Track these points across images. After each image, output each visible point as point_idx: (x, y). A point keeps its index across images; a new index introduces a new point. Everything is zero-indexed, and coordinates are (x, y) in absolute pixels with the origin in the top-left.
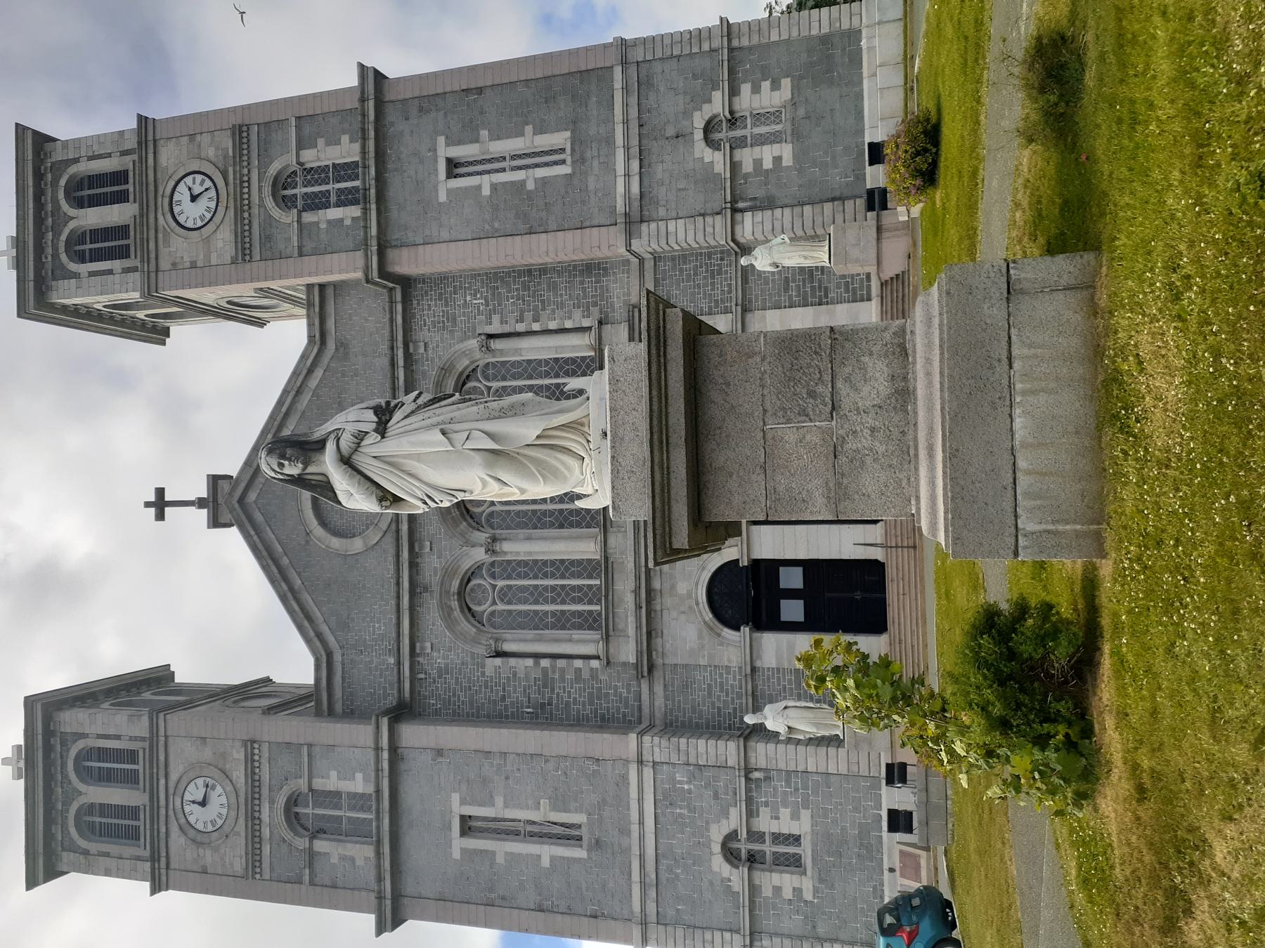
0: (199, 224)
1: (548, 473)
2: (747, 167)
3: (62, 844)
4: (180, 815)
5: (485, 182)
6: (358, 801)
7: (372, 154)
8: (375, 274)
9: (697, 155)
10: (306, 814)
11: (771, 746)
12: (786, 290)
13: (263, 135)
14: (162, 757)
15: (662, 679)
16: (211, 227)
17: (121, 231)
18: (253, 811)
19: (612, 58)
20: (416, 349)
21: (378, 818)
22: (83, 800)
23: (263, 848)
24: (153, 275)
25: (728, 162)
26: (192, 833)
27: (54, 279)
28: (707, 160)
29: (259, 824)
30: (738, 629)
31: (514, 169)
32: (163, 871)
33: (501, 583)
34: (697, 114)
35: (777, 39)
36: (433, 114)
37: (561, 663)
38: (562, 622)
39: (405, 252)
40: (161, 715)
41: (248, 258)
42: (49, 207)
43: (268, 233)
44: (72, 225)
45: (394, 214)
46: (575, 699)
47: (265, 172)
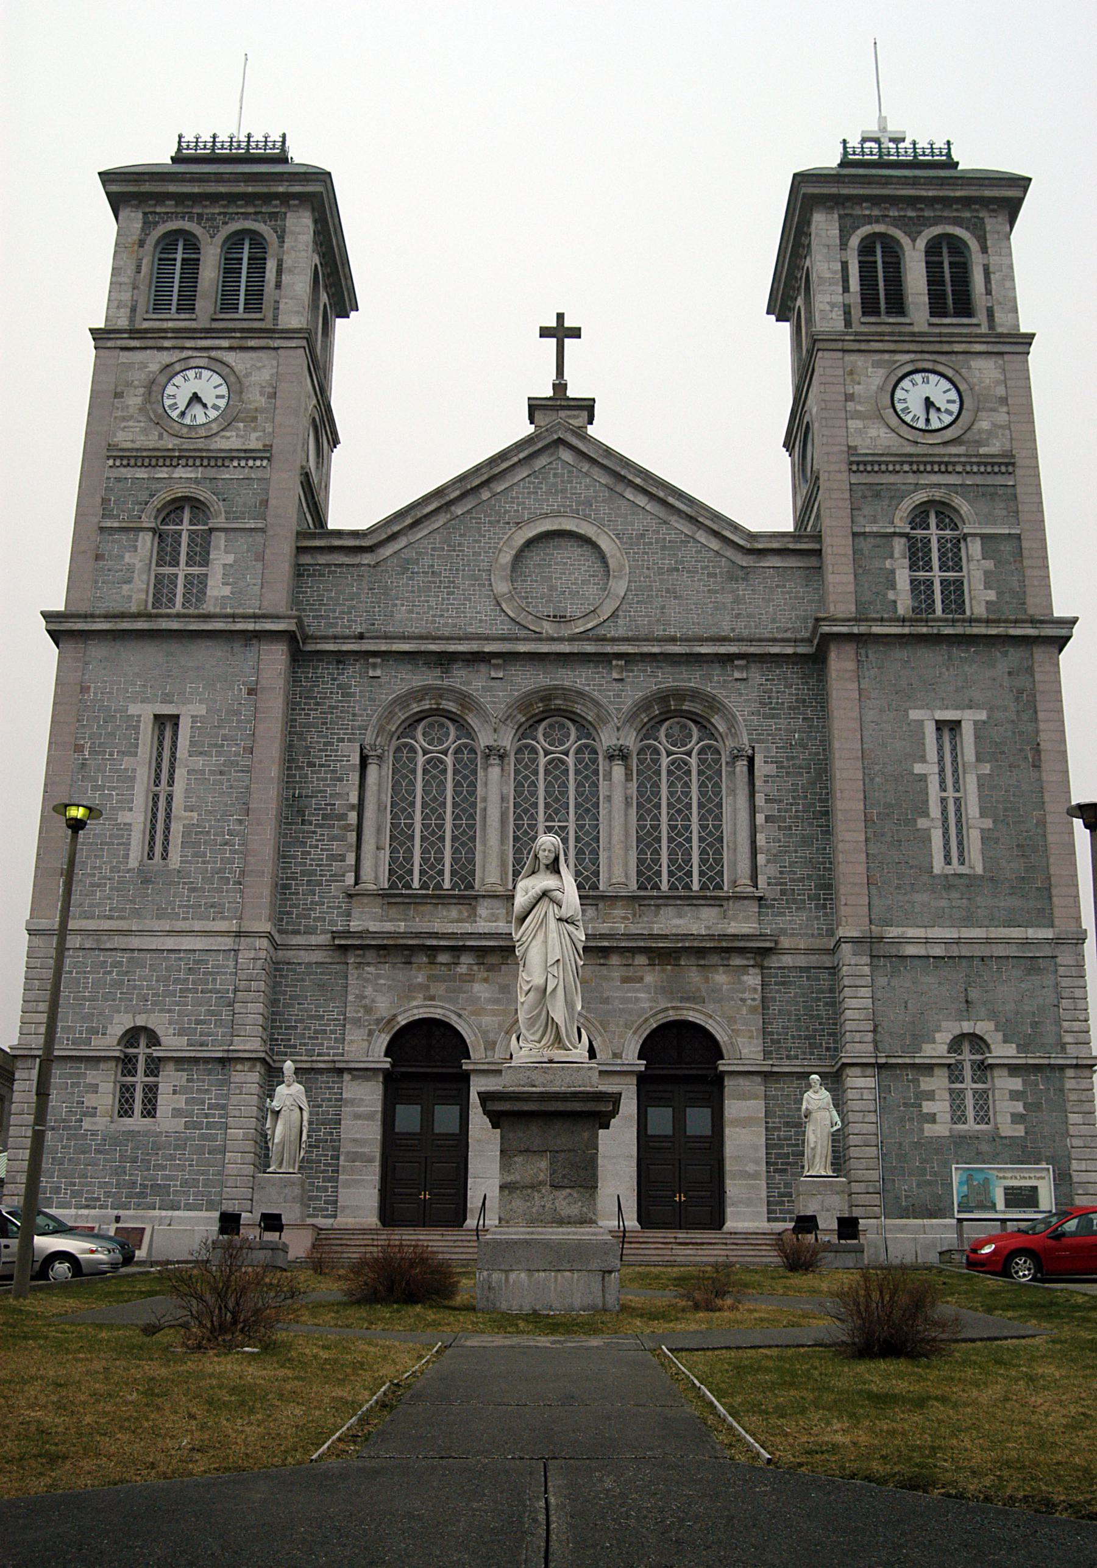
0: (899, 407)
1: (532, 1022)
2: (927, 1083)
3: (151, 213)
4: (182, 365)
5: (929, 768)
6: (197, 586)
7: (969, 631)
8: (826, 629)
9: (944, 1024)
10: (182, 521)
11: (255, 1089)
12: (787, 1124)
13: (1000, 491)
14: (251, 343)
15: (328, 960)
16: (894, 421)
17: (897, 304)
18: (188, 458)
19: (1062, 926)
20: (740, 668)
21: (178, 616)
23: (143, 469)
24: (839, 345)
25: (934, 1061)
26: (162, 379)
27: (840, 217)
28: (937, 1036)
29: (171, 465)
30: (386, 1055)
31: (943, 800)
32: (119, 343)
33: (449, 760)
34: (991, 1026)
35: (1071, 1122)
36: (1012, 706)
37: (352, 837)
38: (400, 837)
39: (851, 665)
40: (304, 343)
41: (854, 468)
43: (882, 494)
44: (905, 241)
45: (900, 654)
46: (309, 853)
47: (957, 493)
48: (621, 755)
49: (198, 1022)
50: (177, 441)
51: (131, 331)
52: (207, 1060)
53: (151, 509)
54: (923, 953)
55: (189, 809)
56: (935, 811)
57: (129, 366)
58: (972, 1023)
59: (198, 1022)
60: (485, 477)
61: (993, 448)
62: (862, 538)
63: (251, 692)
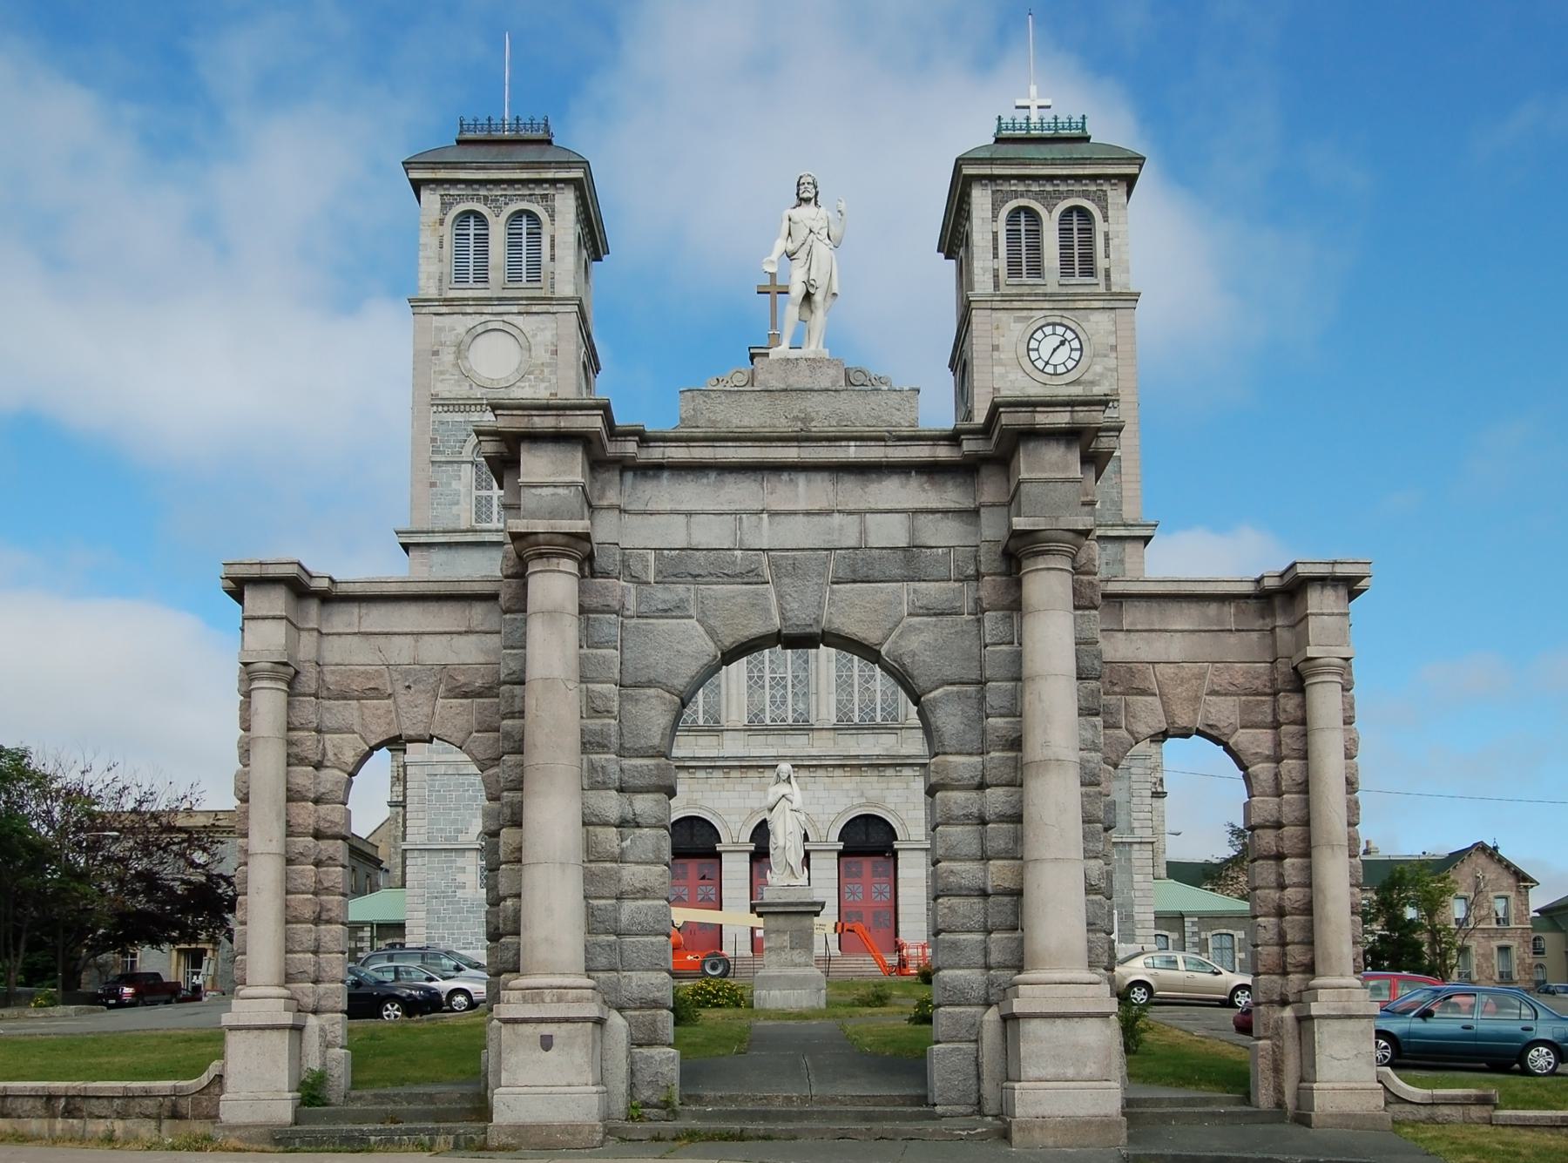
3: (446, 195)
14: (535, 309)
17: (1036, 269)
22: (491, 218)
24: (989, 305)
27: (994, 192)
42: (1063, 188)
44: (1043, 212)
50: (484, 390)
57: (440, 329)
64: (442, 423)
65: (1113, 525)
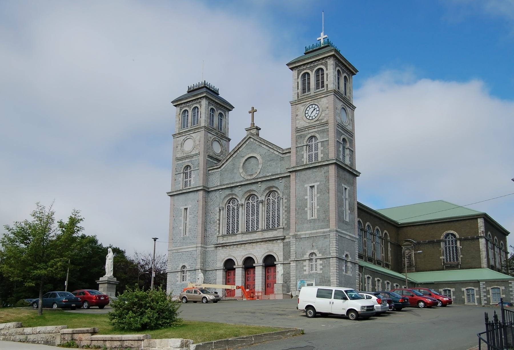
2: (305, 263)
12: (287, 273)
14: (196, 131)
24: (295, 104)
28: (307, 253)
36: (325, 180)
37: (218, 226)
45: (304, 172)
47: (316, 133)
48: (262, 202)
49: (192, 264)
51: (179, 134)
52: (193, 270)
53: (182, 169)
54: (305, 237)
55: (189, 225)
56: (308, 206)
58: (313, 250)
59: (192, 264)
60: (237, 148)
61: (325, 120)
62: (298, 148)
63: (198, 201)
64: (178, 164)
65: (324, 161)
